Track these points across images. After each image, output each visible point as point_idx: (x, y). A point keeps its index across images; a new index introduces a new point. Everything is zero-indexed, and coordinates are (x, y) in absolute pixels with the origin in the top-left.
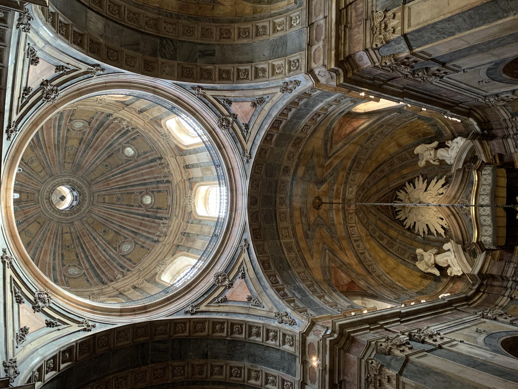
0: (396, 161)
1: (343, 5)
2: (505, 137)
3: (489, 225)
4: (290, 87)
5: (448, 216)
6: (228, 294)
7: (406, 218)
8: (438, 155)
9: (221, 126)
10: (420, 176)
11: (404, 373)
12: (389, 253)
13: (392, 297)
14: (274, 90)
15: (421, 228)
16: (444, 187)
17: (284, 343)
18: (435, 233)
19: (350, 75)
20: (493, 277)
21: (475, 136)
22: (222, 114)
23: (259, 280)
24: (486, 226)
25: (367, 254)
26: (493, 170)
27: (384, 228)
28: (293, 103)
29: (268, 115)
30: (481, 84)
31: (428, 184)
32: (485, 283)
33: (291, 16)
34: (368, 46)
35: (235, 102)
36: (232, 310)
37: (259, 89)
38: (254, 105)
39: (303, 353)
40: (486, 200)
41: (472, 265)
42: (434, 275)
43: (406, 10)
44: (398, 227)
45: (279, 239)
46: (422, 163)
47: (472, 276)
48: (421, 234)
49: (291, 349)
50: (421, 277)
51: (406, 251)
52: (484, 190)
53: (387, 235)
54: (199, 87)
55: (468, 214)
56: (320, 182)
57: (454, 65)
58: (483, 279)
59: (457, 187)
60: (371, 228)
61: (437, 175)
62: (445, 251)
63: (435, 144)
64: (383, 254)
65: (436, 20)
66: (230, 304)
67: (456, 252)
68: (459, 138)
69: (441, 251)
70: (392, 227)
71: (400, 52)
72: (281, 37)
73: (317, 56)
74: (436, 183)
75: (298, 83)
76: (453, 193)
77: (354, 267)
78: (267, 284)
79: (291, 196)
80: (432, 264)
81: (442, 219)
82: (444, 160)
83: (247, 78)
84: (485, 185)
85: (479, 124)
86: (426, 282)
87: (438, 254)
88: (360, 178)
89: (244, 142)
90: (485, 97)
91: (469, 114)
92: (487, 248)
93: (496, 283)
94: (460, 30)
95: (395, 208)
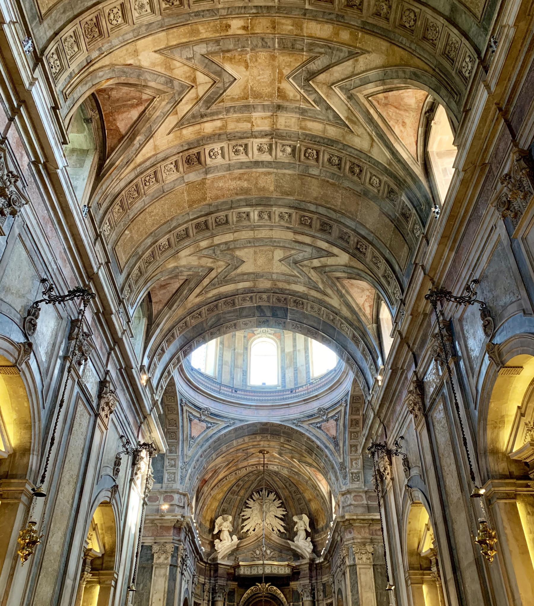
2: (311, 578)
5: (256, 535)
6: (196, 421)
9: (320, 410)
13: (198, 512)
14: (342, 456)
15: (247, 513)
17: (168, 473)
18: (244, 524)
19: (341, 524)
20: (216, 571)
21: (312, 560)
22: (329, 413)
23: (207, 440)
26: (288, 574)
27: (246, 486)
29: (326, 447)
31: (281, 519)
34: (355, 541)
35: (337, 424)
36: (185, 429)
37: (344, 446)
38: (334, 438)
39: (166, 492)
40: (268, 571)
41: (223, 558)
42: (213, 531)
44: (247, 496)
45: (236, 439)
46: (295, 519)
47: (215, 559)
48: (243, 514)
49: (165, 480)
50: (212, 519)
54: (347, 405)
55: (258, 559)
56: (280, 454)
58: (214, 565)
59: (277, 541)
60: (246, 478)
61: (287, 524)
62: (231, 537)
63: (309, 530)
64: (225, 489)
65: (359, 585)
66: (189, 425)
67: (232, 546)
68: (312, 547)
69: (231, 534)
73: (358, 498)
75: (345, 478)
76: (273, 539)
78: (204, 448)
79: (269, 441)
81: (254, 530)
82: (297, 534)
83: (351, 439)
85: (320, 563)
86: (208, 525)
87: (229, 531)
88: (285, 472)
89: (309, 422)
91: (325, 559)
93: (212, 572)
94: (353, 595)
95: (262, 491)
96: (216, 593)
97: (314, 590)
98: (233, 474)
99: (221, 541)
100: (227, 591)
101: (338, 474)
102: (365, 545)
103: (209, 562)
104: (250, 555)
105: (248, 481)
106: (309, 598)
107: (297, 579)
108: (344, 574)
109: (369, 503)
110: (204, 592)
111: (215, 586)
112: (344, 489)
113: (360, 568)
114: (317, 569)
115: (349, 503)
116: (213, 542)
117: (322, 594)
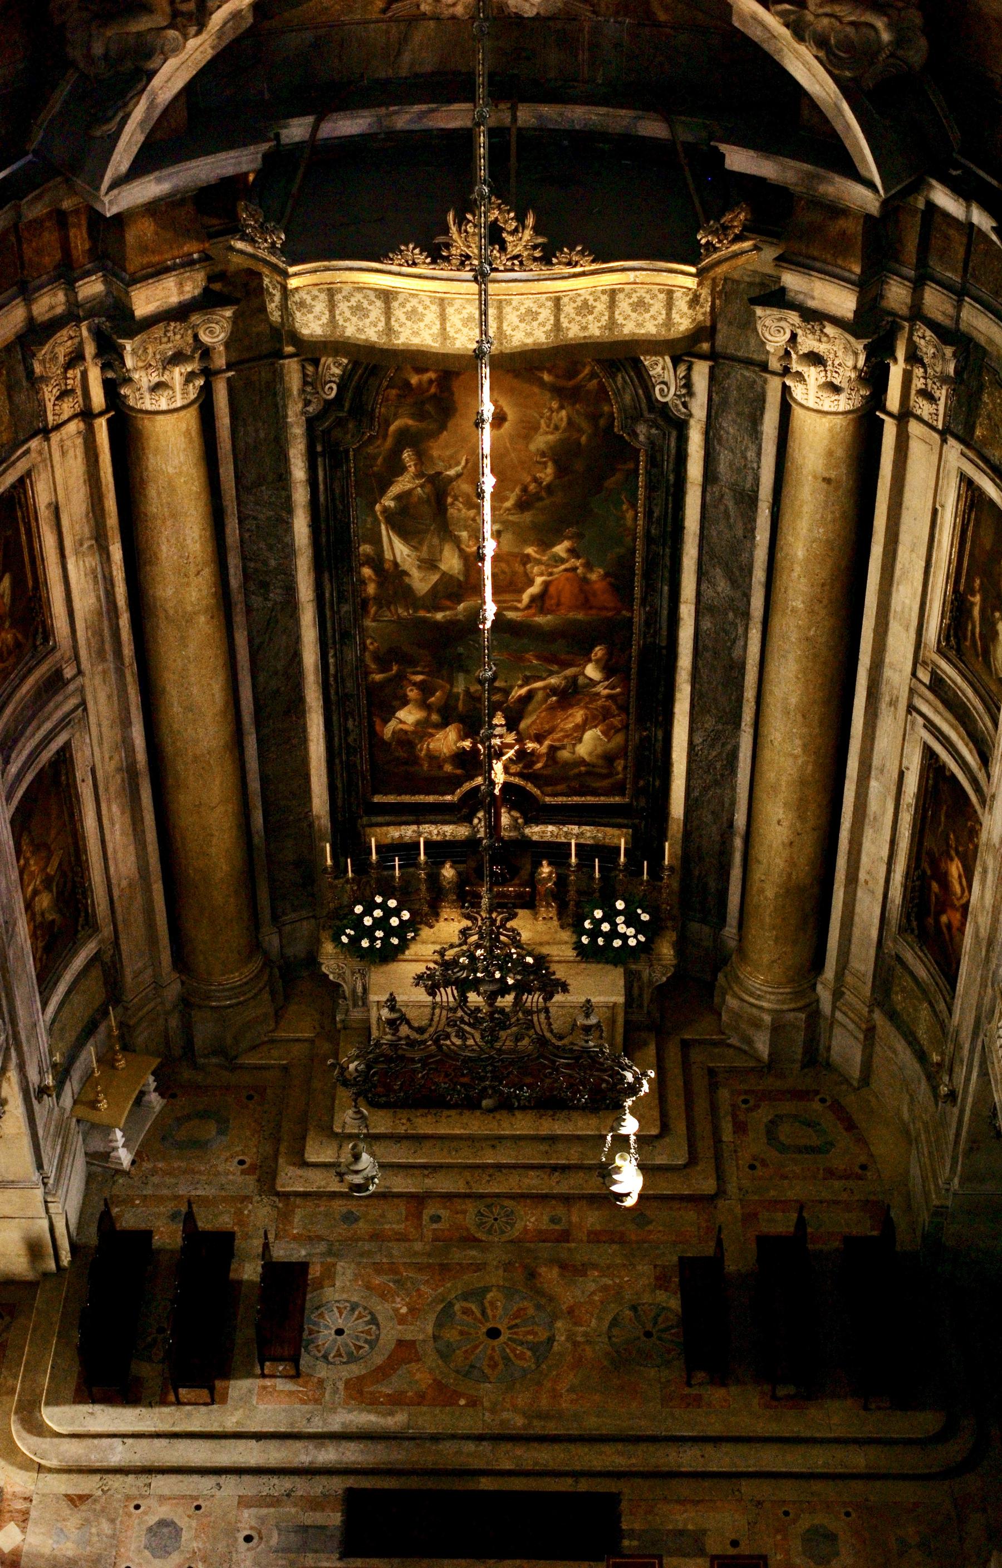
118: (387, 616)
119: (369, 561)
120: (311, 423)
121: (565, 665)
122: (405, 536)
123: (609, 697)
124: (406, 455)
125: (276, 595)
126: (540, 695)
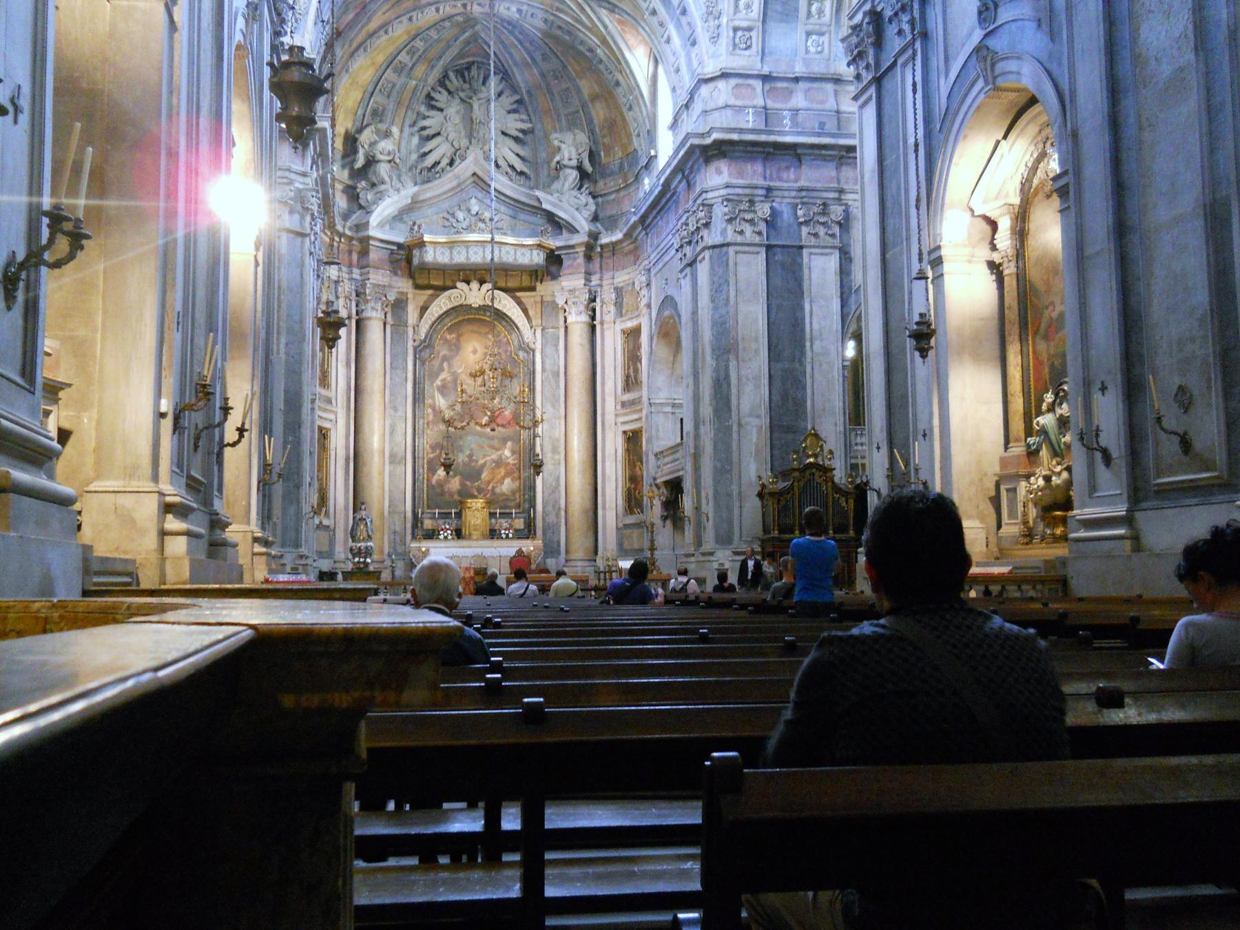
0: (564, 86)
1: (799, 151)
2: (588, 274)
3: (451, 258)
4: (712, 23)
7: (450, 92)
8: (568, 171)
10: (530, 125)
11: (291, 235)
12: (383, 67)
16: (509, 170)
20: (364, 253)
21: (594, 236)
24: (451, 253)
25: (385, 37)
26: (537, 265)
28: (684, 12)
30: (664, 282)
31: (516, 139)
32: (354, 242)
33: (827, 36)
41: (381, 225)
43: (757, 249)
51: (388, 97)
52: (508, 253)
53: (418, 60)
57: (686, 275)
59: (508, 193)
60: (433, 34)
64: (380, 59)
65: (732, 289)
70: (433, 67)
71: (710, 232)
72: (797, 10)
73: (743, 90)
74: (517, 155)
75: (715, 39)
77: (366, 28)
80: (373, 157)
84: (515, 254)
90: (649, 270)
91: (628, 235)
92: (414, 252)
93: (355, 257)
94: (715, 308)
95: (468, 69)
96: (367, 301)
97: (594, 300)
98: (405, 19)
99: (373, 185)
100: (392, 297)
101: (699, 30)
102: (752, 202)
103: (348, 233)
104: (441, 222)
105: (438, 41)
106: (585, 318)
107: (555, 277)
108: (691, 264)
109: (770, 104)
110: (337, 298)
111: (364, 286)
112: (711, 69)
113: (737, 253)
114: (601, 256)
115: (721, 103)
116: (354, 188)
117: (612, 308)
118: (436, 429)
119: (430, 406)
120: (415, 348)
121: (497, 450)
122: (443, 395)
123: (514, 465)
124: (445, 365)
125: (400, 413)
126: (488, 464)
